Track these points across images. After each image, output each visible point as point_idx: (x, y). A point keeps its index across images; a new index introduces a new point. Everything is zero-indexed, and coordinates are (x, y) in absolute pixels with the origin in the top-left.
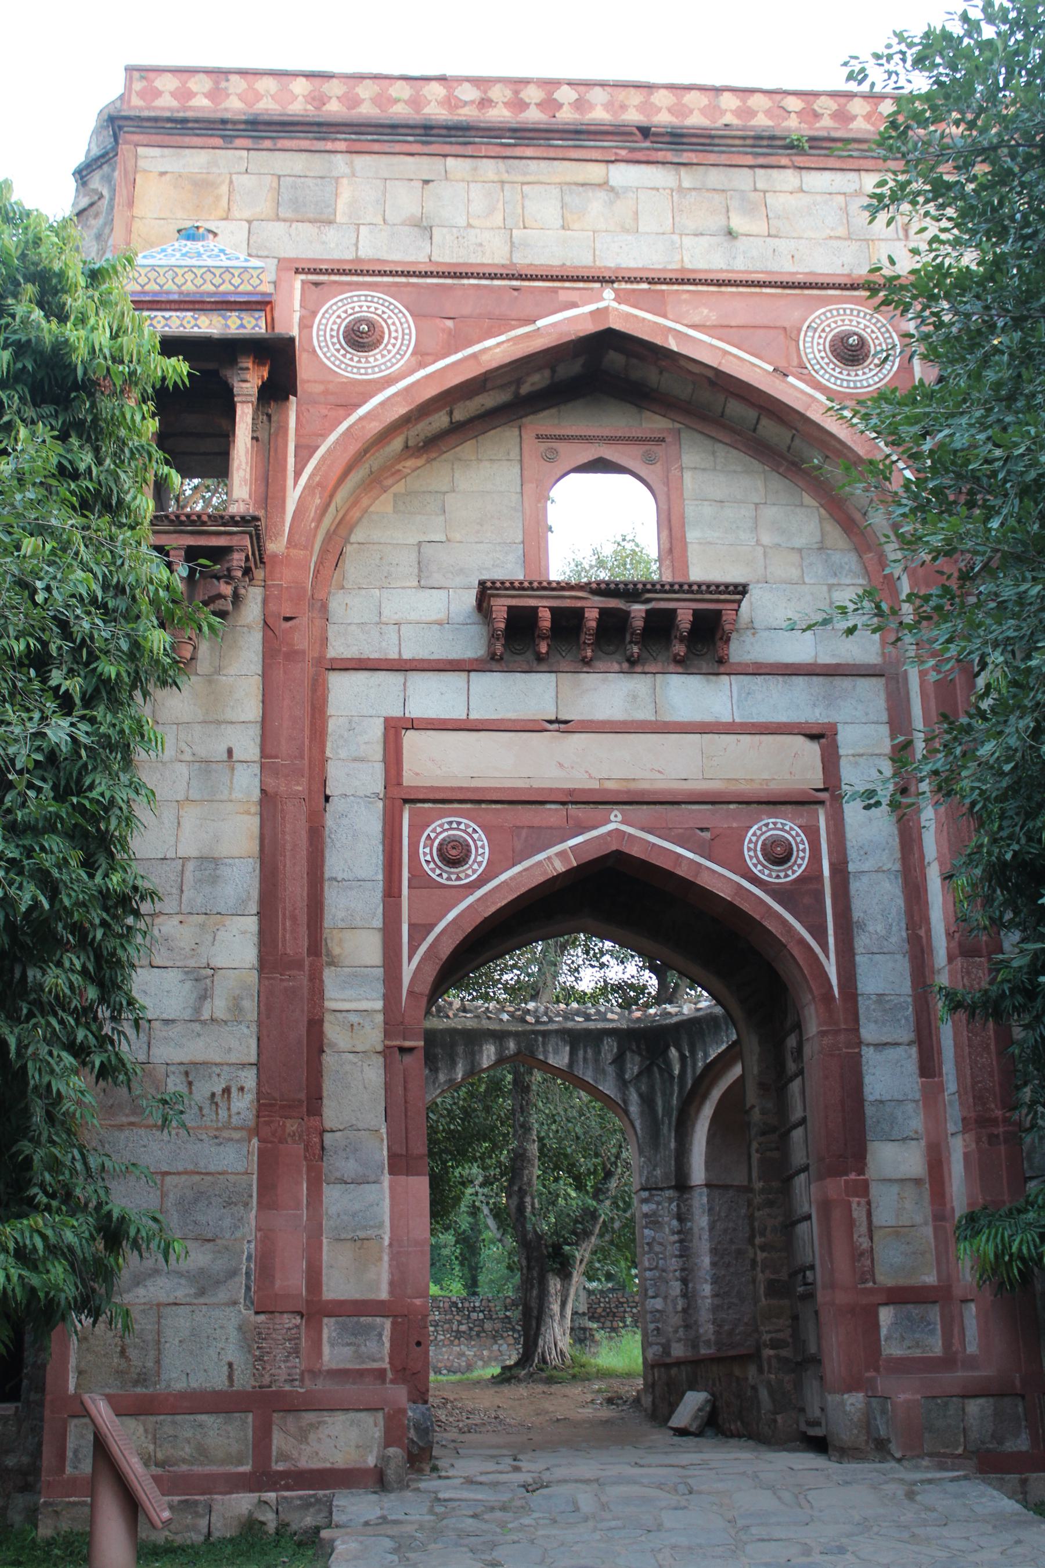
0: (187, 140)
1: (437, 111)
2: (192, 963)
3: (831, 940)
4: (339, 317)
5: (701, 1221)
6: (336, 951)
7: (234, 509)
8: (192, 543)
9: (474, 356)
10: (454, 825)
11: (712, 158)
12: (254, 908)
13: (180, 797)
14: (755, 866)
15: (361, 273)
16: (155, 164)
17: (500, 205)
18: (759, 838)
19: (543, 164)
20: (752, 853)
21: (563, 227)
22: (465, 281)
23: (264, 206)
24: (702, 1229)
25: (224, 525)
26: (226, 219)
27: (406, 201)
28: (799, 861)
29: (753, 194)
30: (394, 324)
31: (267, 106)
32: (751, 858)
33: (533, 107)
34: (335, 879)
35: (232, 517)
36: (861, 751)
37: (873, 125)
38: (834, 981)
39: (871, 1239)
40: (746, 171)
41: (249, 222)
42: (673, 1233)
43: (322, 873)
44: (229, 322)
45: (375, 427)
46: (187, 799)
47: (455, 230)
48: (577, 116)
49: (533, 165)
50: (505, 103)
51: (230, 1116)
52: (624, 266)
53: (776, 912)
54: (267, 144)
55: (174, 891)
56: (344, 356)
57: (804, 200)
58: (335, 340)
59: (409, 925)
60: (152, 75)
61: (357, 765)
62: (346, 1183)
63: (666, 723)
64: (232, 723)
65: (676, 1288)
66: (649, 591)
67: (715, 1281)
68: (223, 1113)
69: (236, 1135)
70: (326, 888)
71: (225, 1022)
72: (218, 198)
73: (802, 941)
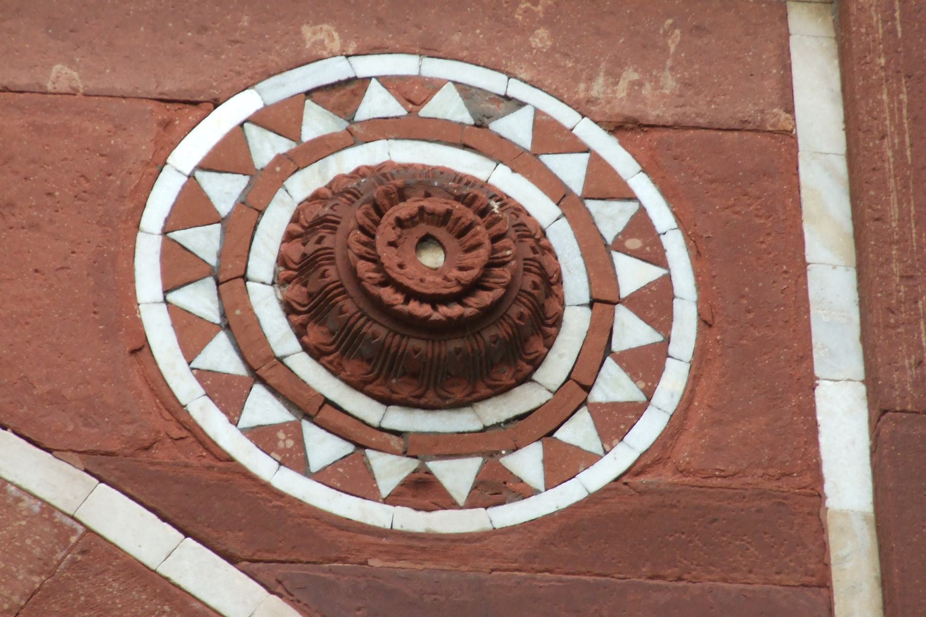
14: (227, 394)
18: (264, 184)
20: (200, 300)
28: (614, 385)
32: (191, 333)
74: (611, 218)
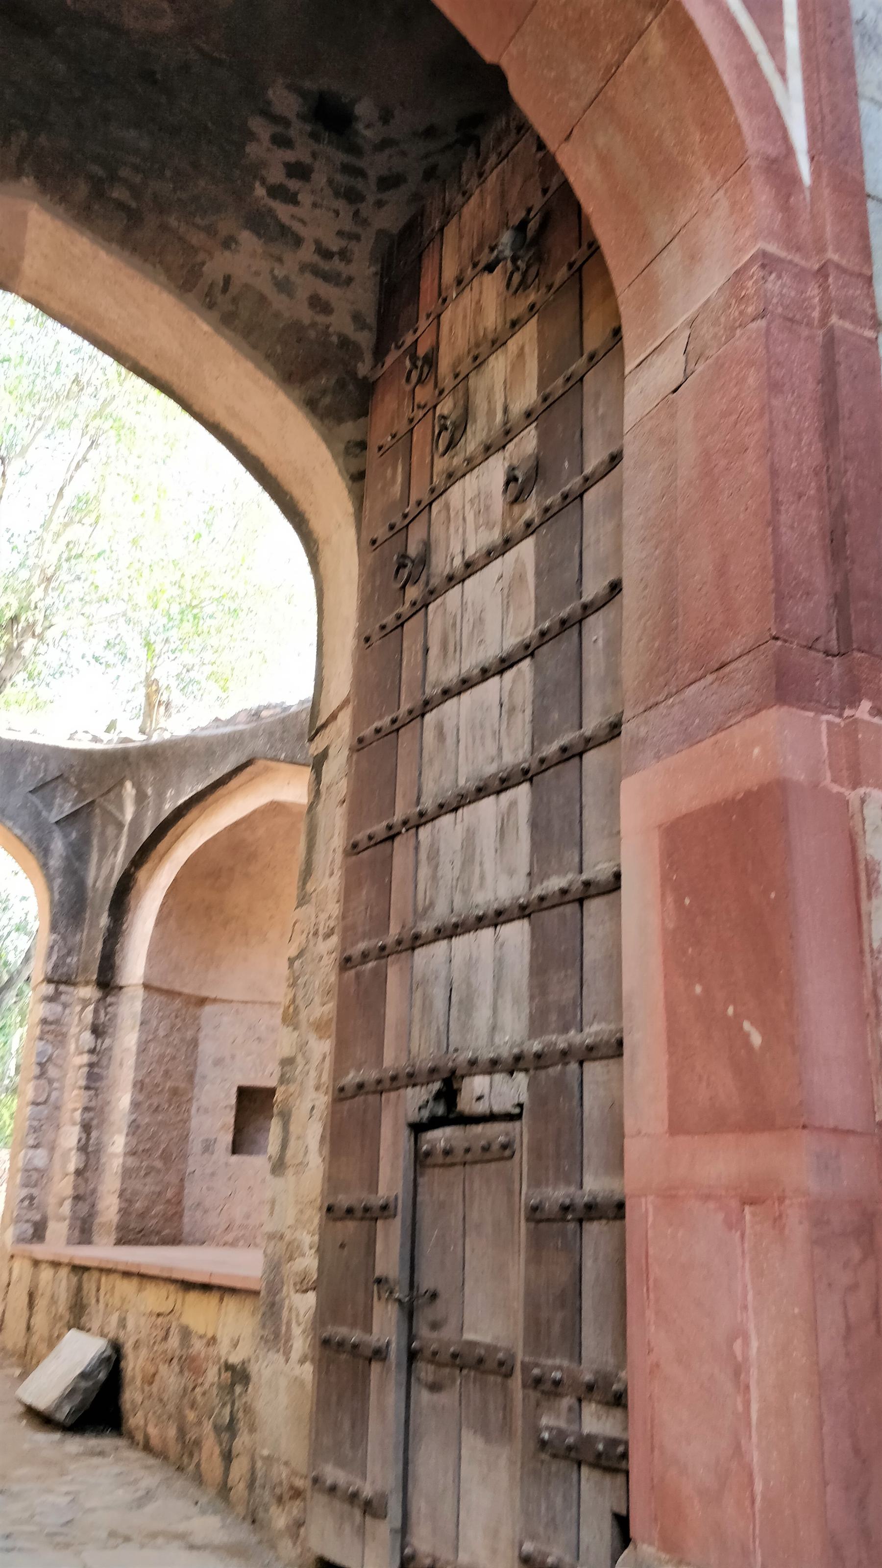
5: (127, 1039)
24: (127, 1050)
42: (81, 1053)
65: (71, 1136)
67: (134, 1128)
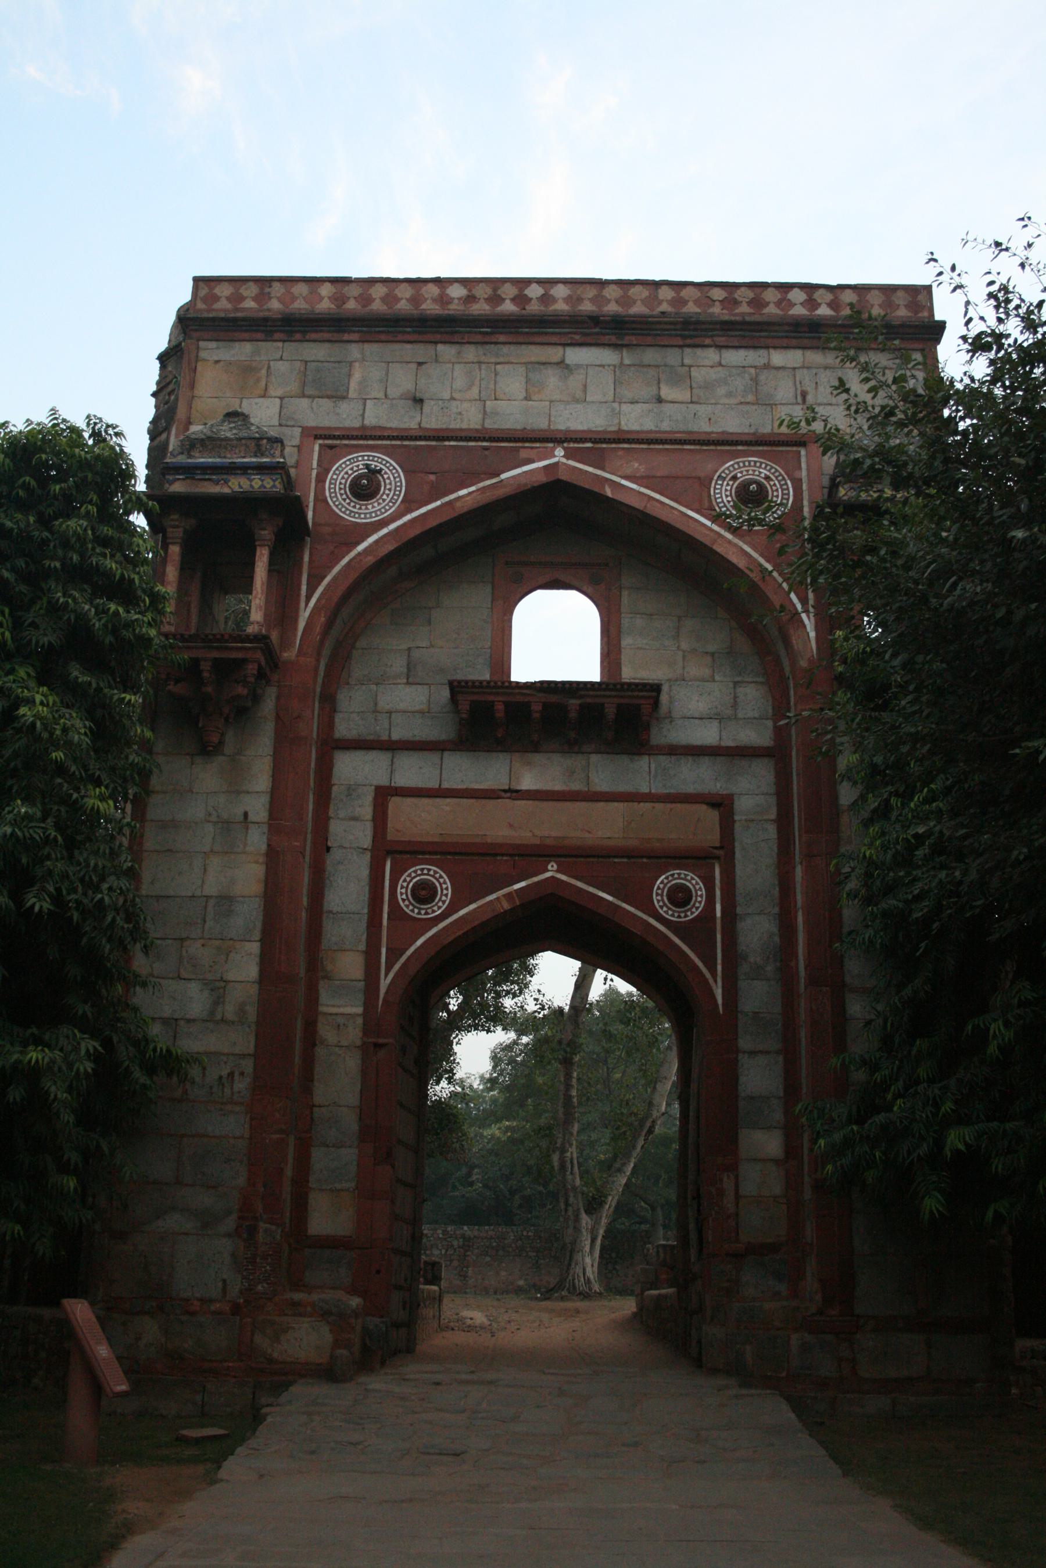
0: (237, 335)
1: (432, 307)
2: (210, 976)
3: (719, 968)
4: (347, 473)
6: (329, 968)
7: (250, 630)
8: (216, 654)
9: (450, 502)
10: (425, 872)
11: (649, 340)
12: (257, 935)
13: (207, 848)
14: (661, 907)
15: (366, 438)
16: (211, 351)
17: (477, 383)
19: (512, 347)
21: (527, 399)
22: (447, 443)
23: (294, 387)
25: (242, 642)
26: (264, 396)
27: (403, 380)
28: (697, 905)
29: (680, 368)
30: (389, 478)
31: (300, 305)
32: (658, 901)
33: (508, 302)
34: (331, 912)
35: (248, 636)
36: (753, 817)
37: (782, 310)
38: (720, 1001)
39: (737, 1205)
40: (677, 349)
41: (281, 398)
43: (322, 906)
44: (253, 483)
45: (370, 560)
46: (212, 851)
47: (440, 402)
48: (542, 308)
49: (505, 349)
50: (486, 299)
51: (233, 1094)
52: (572, 428)
53: (676, 945)
54: (298, 336)
55: (199, 921)
56: (349, 504)
57: (721, 372)
58: (342, 492)
59: (387, 949)
60: (213, 284)
61: (352, 823)
62: (328, 1146)
63: (596, 793)
64: (248, 792)
66: (582, 689)
68: (227, 1091)
69: (237, 1109)
70: (324, 918)
71: (233, 1023)
72: (258, 380)
73: (696, 968)
74: (697, 887)
